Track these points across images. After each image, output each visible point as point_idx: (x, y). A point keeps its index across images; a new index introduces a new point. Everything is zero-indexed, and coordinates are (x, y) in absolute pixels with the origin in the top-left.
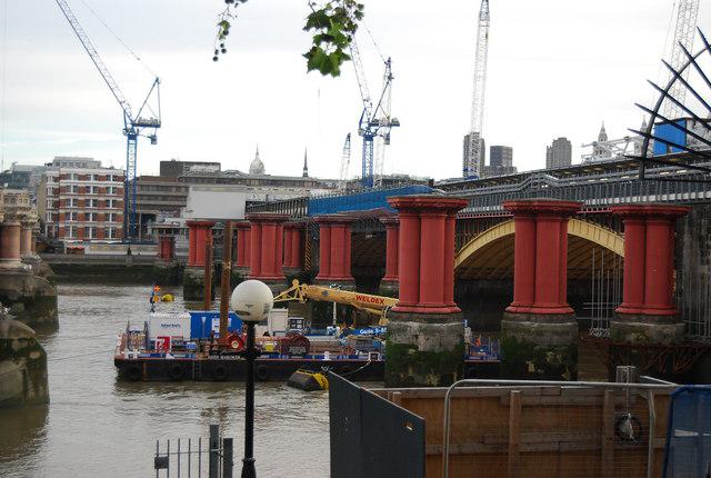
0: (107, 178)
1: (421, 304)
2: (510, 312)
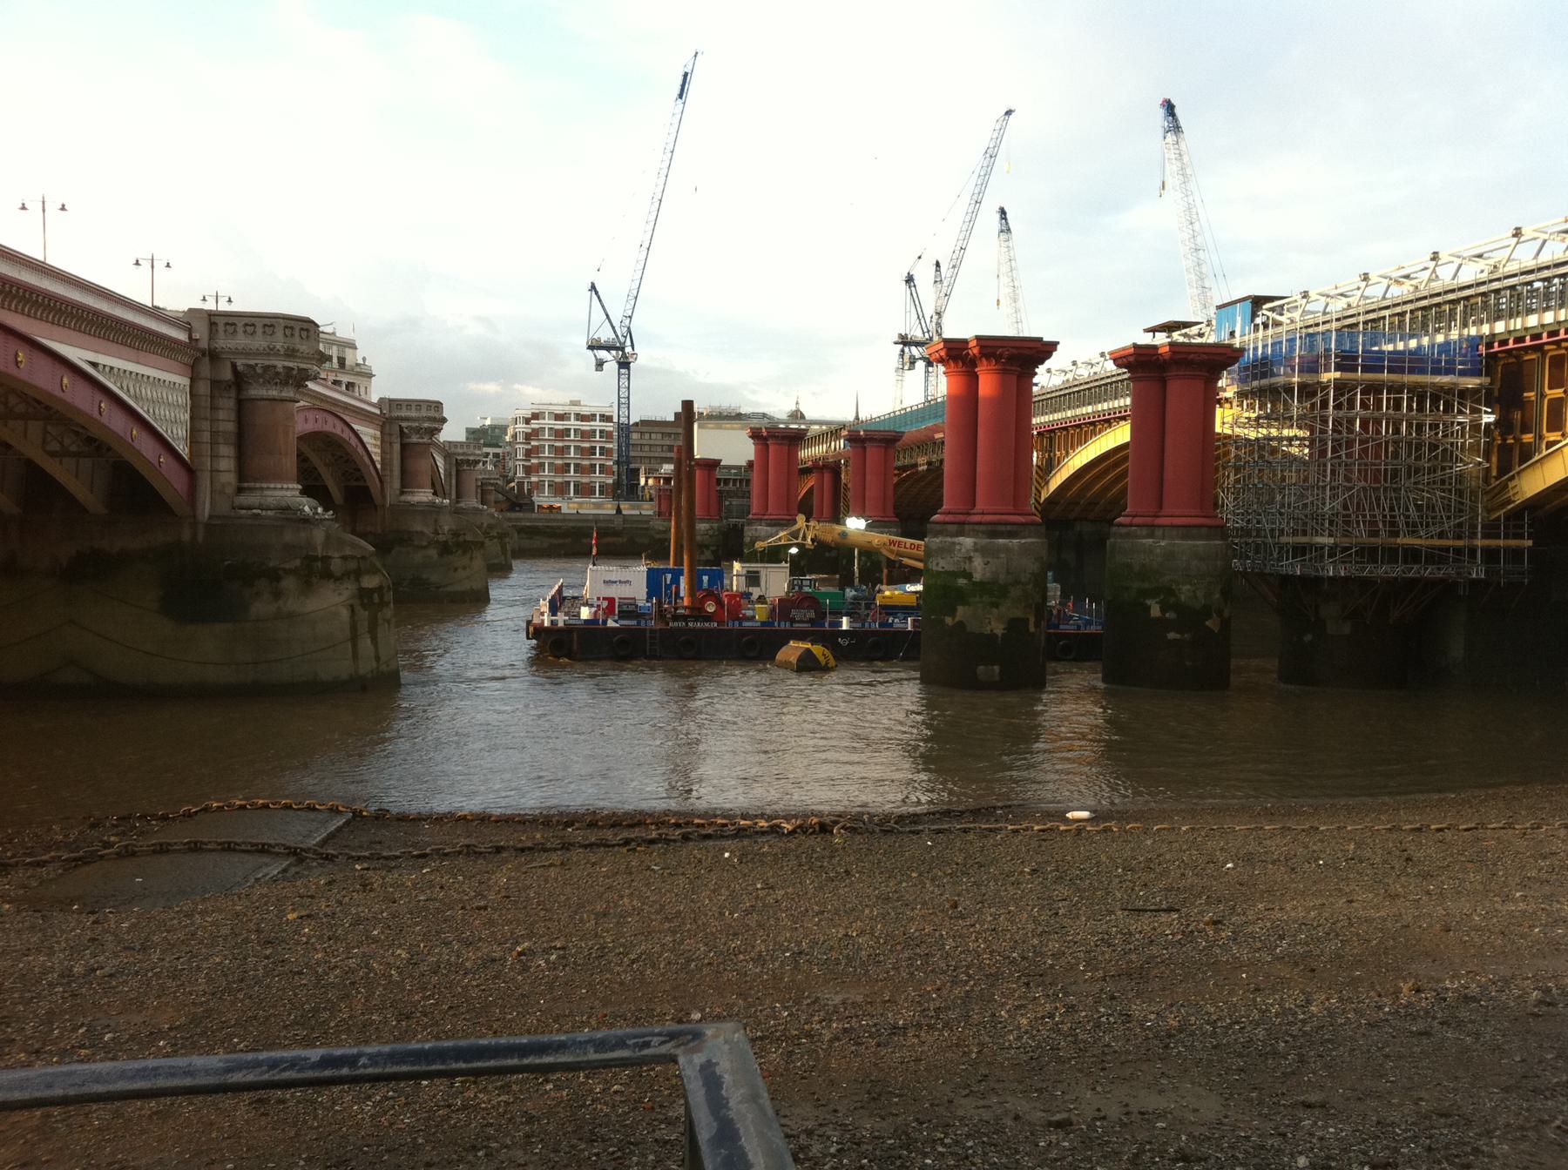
0: (592, 417)
1: (980, 506)
2: (1121, 525)
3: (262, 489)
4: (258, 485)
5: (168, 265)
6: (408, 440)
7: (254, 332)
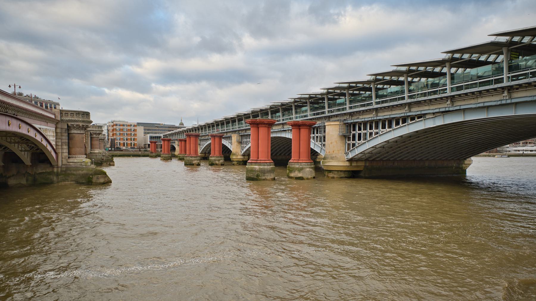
1: (260, 159)
3: (76, 157)
4: (75, 156)
5: (20, 87)
6: (93, 136)
7: (73, 115)
